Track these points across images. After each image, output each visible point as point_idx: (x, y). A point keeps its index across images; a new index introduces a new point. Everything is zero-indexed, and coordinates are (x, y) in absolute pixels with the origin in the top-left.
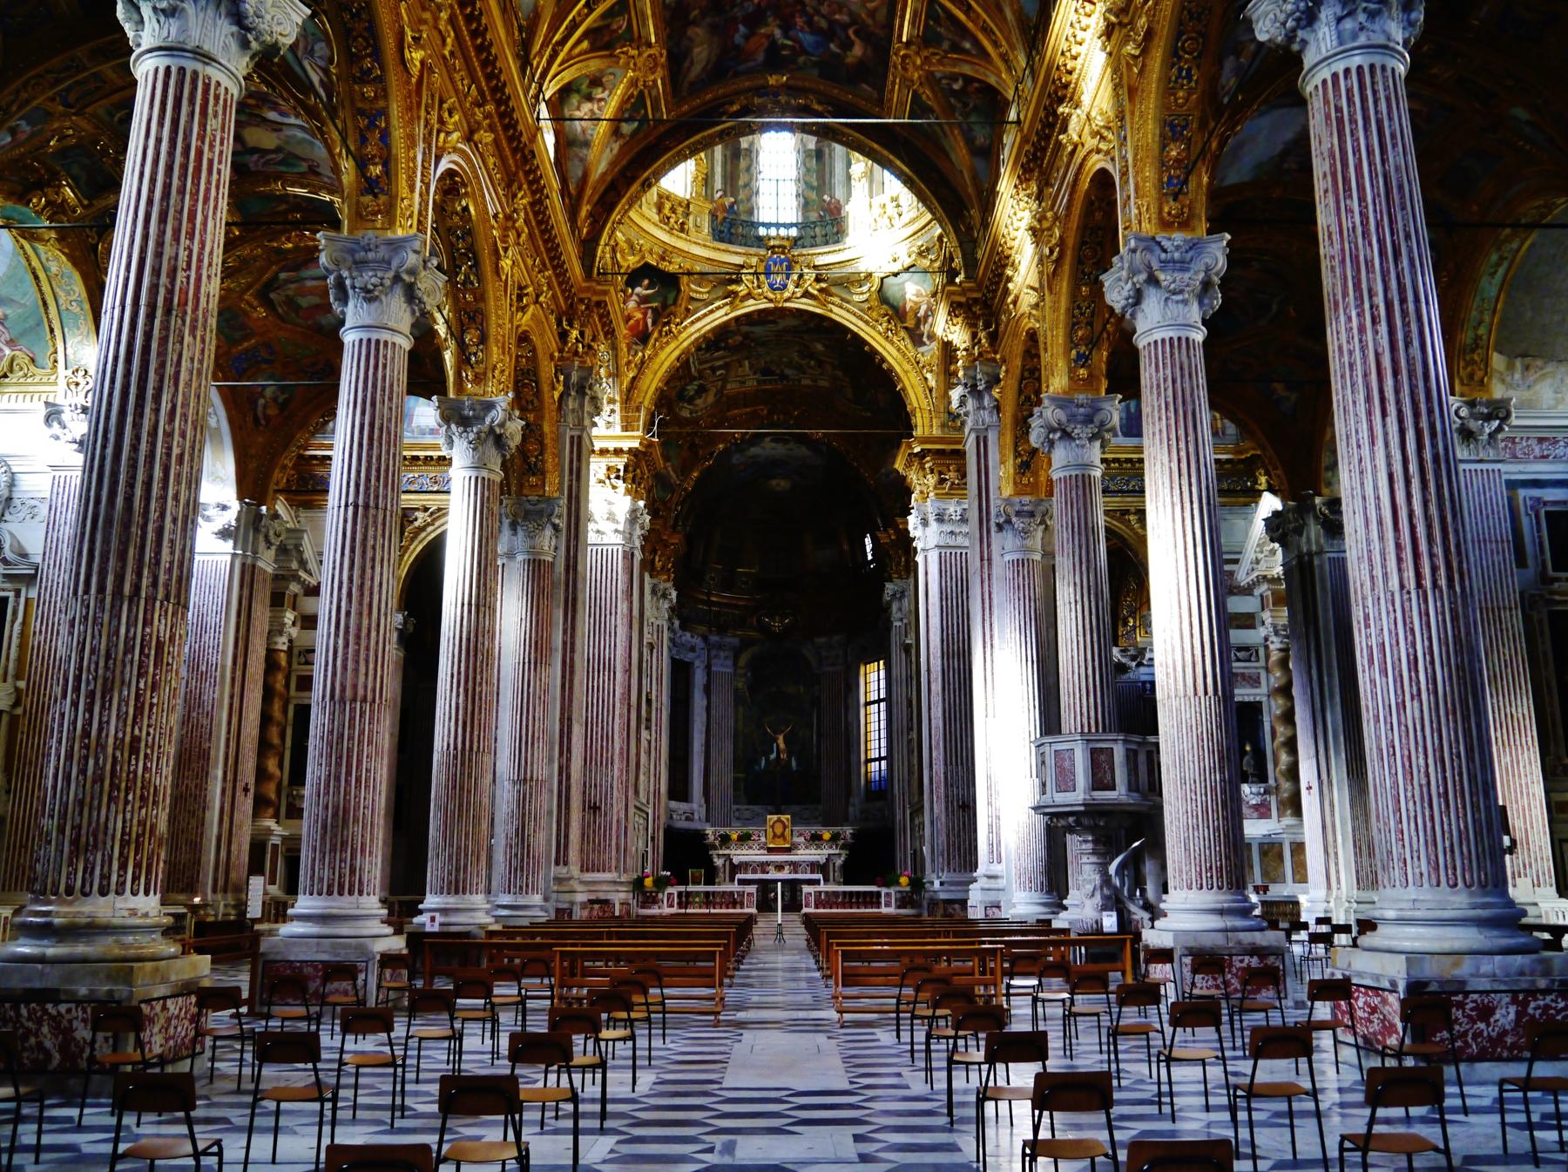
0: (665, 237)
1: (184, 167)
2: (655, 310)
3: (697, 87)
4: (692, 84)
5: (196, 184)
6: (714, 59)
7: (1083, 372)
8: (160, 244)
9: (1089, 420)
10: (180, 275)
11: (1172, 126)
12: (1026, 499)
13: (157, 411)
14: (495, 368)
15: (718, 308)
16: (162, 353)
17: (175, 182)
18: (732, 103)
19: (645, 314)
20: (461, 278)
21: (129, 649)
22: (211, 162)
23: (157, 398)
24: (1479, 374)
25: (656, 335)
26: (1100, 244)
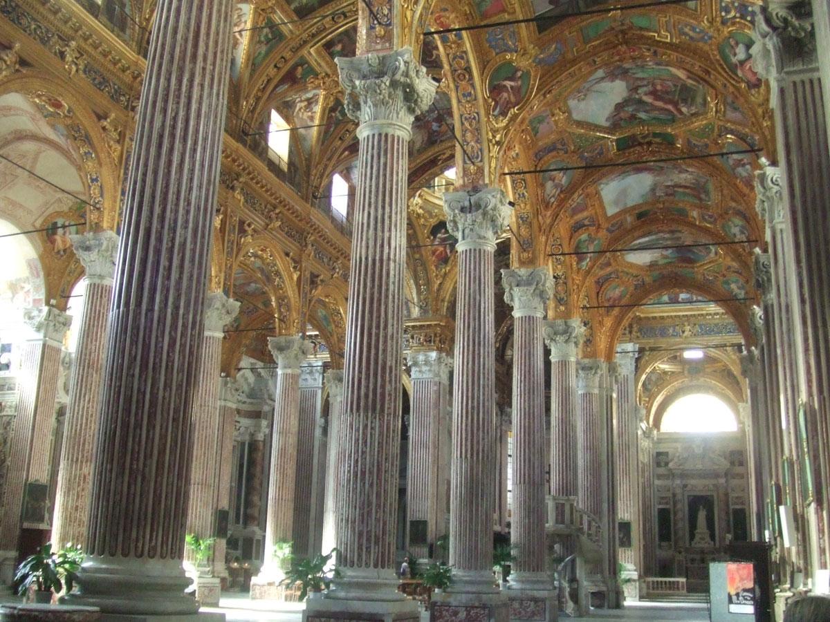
1: (94, 317)
3: (420, 152)
4: (418, 151)
5: (98, 322)
6: (426, 139)
7: (562, 308)
8: (87, 345)
9: (565, 332)
10: (93, 355)
11: (522, 218)
13: (84, 401)
14: (294, 322)
16: (87, 381)
17: (92, 323)
18: (444, 154)
19: (445, 248)
20: (276, 283)
21: (75, 479)
22: (103, 313)
23: (85, 396)
25: (452, 258)
26: (560, 245)
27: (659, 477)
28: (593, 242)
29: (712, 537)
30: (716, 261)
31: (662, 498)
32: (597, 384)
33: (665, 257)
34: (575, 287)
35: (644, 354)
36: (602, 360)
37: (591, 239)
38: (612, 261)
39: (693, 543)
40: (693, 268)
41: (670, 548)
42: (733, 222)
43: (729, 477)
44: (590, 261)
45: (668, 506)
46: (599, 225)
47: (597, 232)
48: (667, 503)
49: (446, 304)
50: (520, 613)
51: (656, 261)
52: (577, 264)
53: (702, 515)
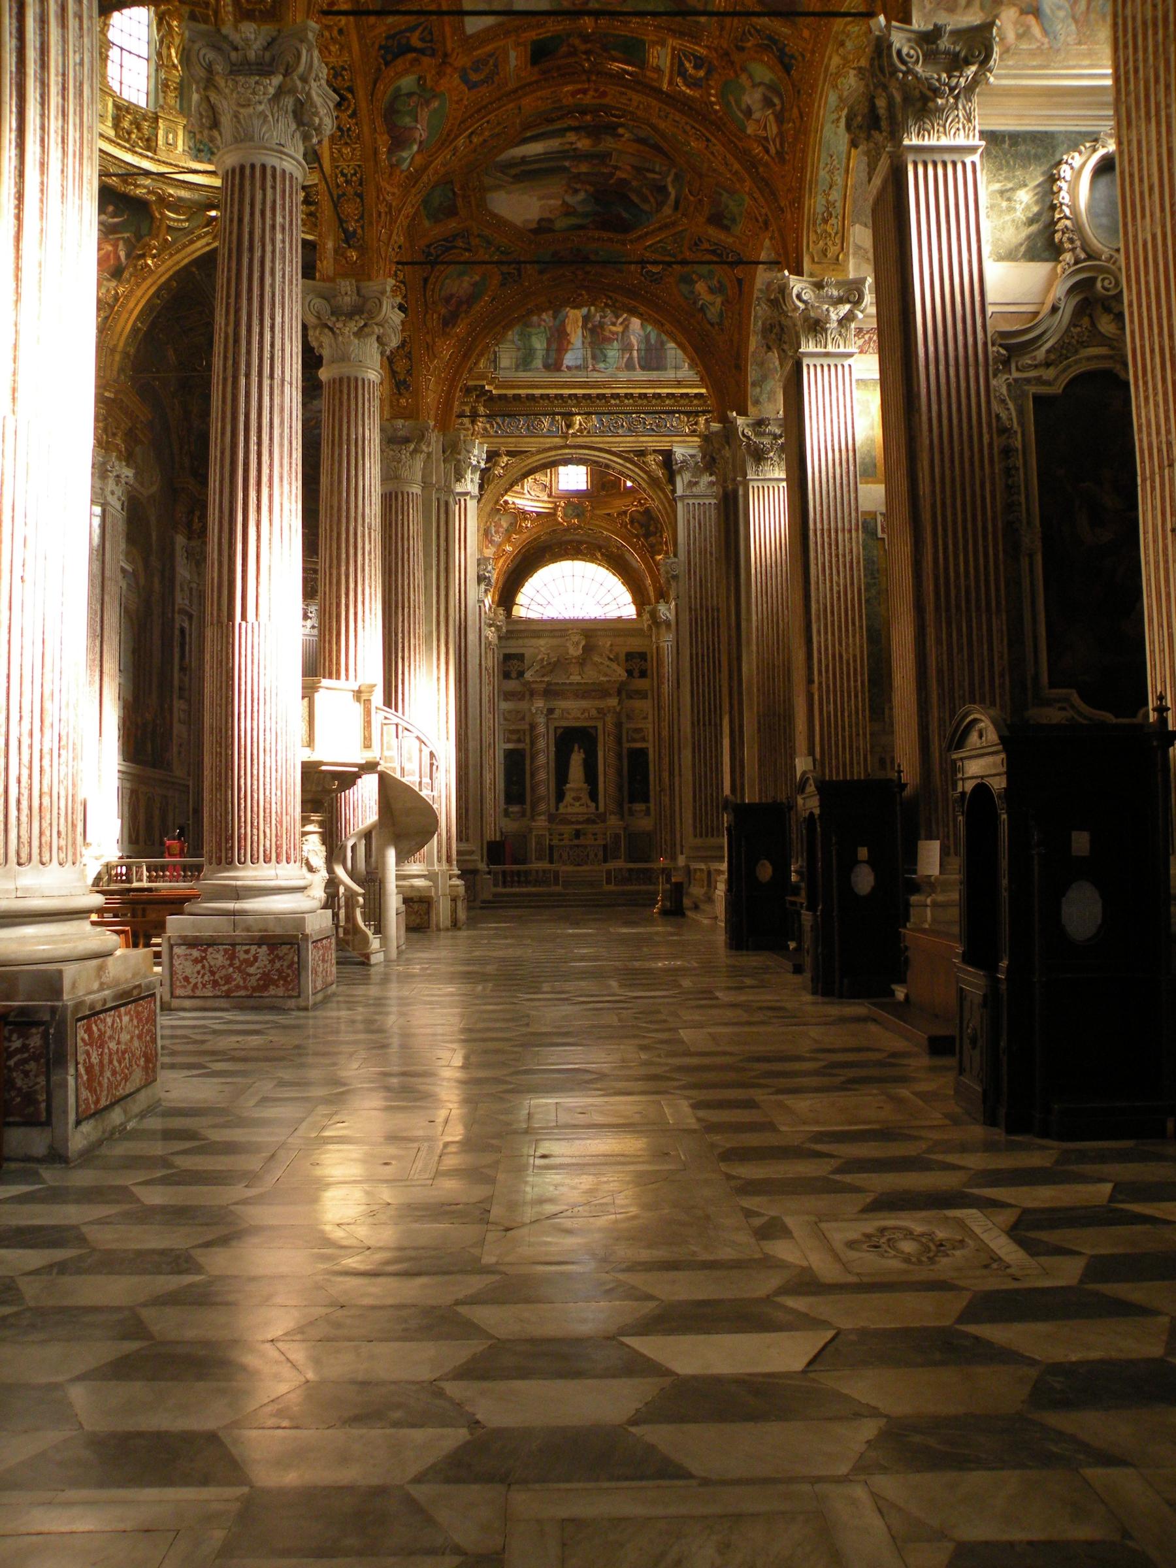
0: (128, 157)
2: (127, 241)
9: (356, 311)
12: (400, 423)
15: (199, 237)
19: (116, 246)
24: (833, 250)
27: (508, 696)
28: (427, 102)
29: (593, 796)
30: (674, 224)
31: (513, 732)
32: (419, 476)
33: (569, 211)
34: (383, 209)
35: (496, 464)
36: (432, 423)
37: (425, 93)
38: (460, 202)
39: (561, 806)
40: (624, 244)
41: (523, 814)
42: (751, 77)
43: (624, 695)
44: (419, 151)
45: (520, 746)
46: (446, 55)
47: (440, 74)
48: (519, 741)
49: (117, 357)
50: (228, 979)
51: (550, 220)
52: (390, 151)
53: (577, 760)
